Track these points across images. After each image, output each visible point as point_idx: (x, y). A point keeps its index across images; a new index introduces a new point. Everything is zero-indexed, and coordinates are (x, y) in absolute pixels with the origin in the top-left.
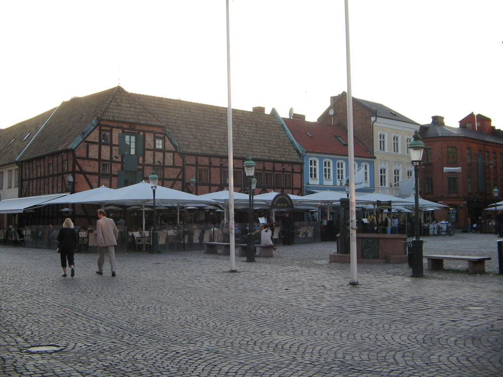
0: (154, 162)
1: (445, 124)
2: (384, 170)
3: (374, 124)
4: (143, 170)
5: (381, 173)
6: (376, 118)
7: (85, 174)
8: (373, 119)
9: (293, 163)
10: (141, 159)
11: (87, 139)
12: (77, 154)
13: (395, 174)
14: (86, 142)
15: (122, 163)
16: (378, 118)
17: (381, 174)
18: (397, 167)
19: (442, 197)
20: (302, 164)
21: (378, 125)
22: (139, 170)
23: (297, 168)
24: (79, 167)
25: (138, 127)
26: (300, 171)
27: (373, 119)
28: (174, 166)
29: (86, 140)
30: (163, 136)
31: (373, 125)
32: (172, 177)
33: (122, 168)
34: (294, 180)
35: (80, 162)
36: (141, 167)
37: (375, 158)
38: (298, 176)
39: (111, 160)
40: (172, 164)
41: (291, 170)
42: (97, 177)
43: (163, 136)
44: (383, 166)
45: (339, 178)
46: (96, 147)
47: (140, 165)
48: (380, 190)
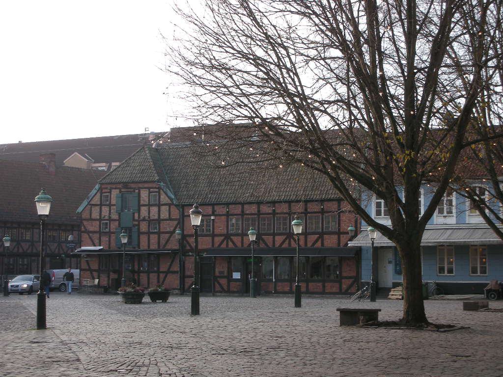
0: (149, 217)
4: (139, 225)
7: (88, 232)
10: (136, 215)
11: (91, 203)
12: (83, 216)
14: (90, 205)
15: (119, 220)
22: (134, 225)
24: (85, 227)
25: (133, 186)
28: (170, 219)
29: (91, 203)
30: (157, 190)
32: (168, 230)
33: (119, 224)
35: (85, 223)
36: (136, 223)
39: (110, 220)
40: (168, 216)
42: (98, 235)
43: (157, 190)
46: (98, 208)
47: (136, 221)
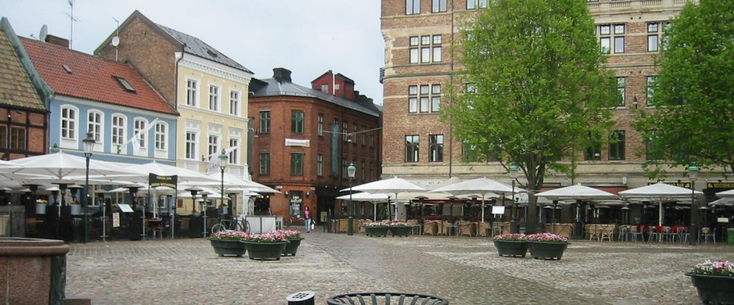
1: (292, 81)
2: (193, 135)
3: (179, 64)
5: (188, 138)
6: (183, 55)
8: (178, 55)
9: (28, 111)
13: (210, 142)
16: (185, 55)
17: (188, 141)
18: (213, 132)
19: (281, 179)
20: (46, 113)
21: (186, 65)
23: (36, 120)
26: (42, 125)
27: (178, 55)
31: (177, 64)
34: (30, 139)
37: (178, 115)
38: (40, 132)
41: (25, 122)
44: (191, 129)
45: (115, 140)
48: (185, 164)
